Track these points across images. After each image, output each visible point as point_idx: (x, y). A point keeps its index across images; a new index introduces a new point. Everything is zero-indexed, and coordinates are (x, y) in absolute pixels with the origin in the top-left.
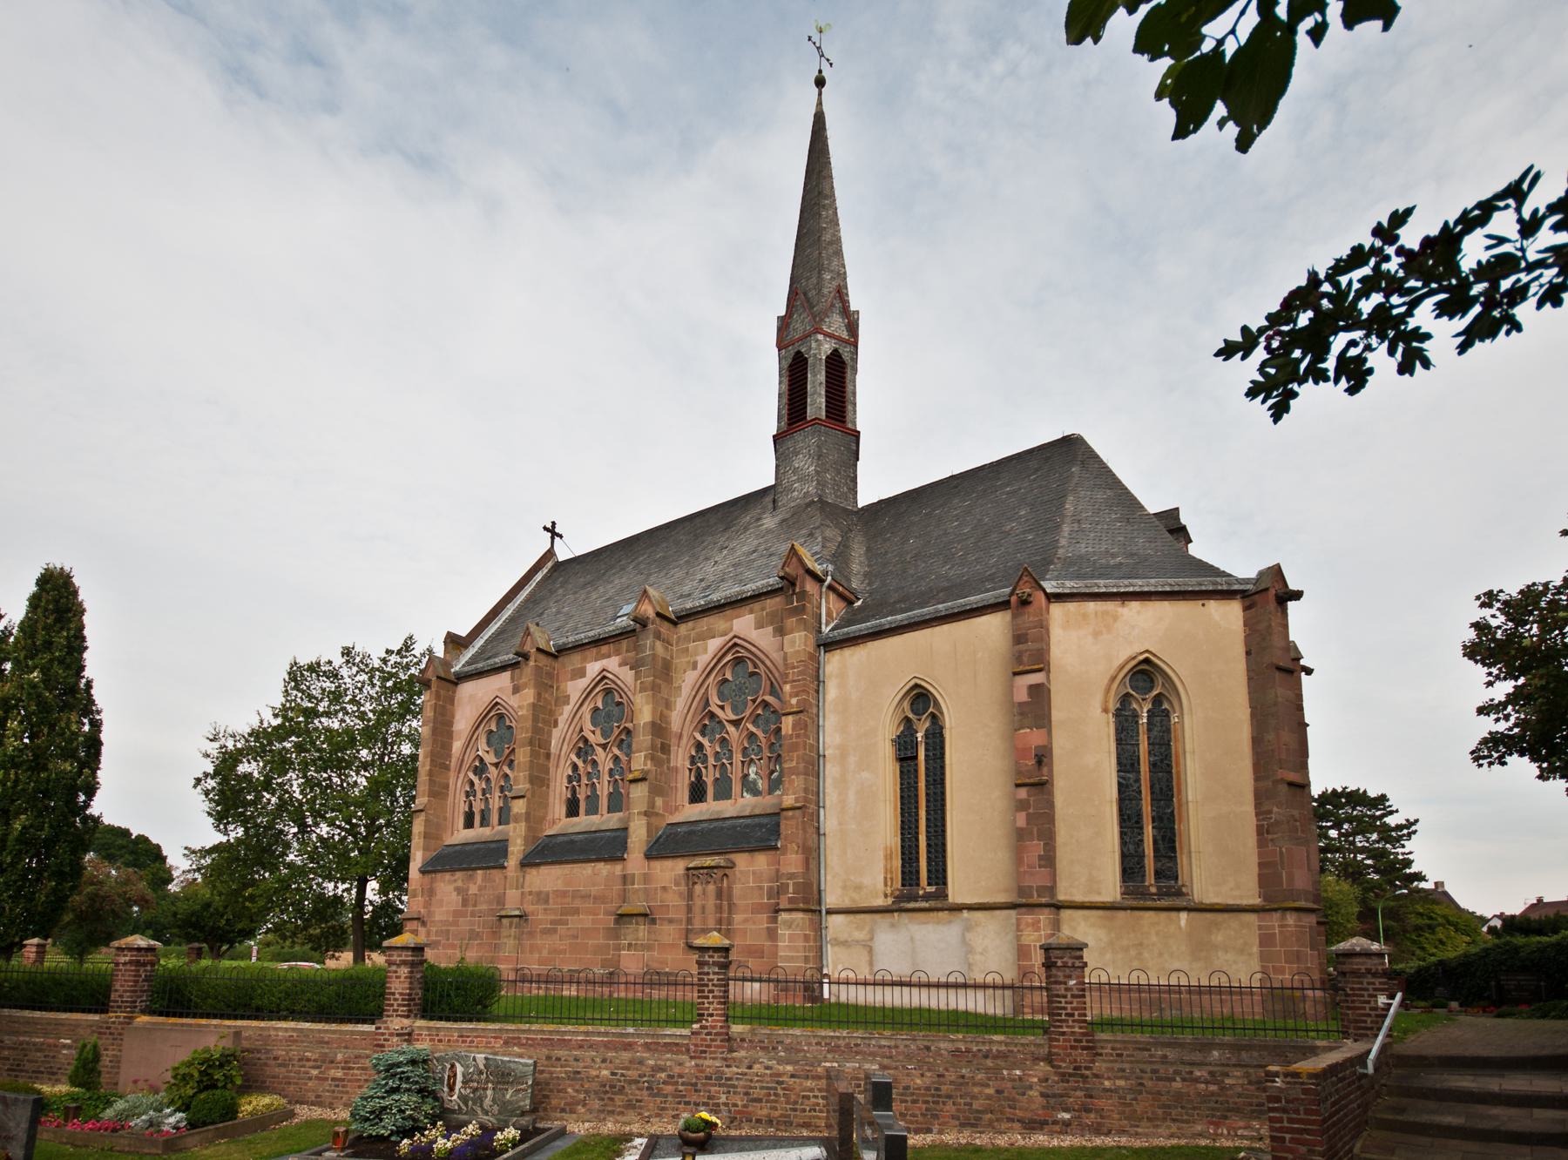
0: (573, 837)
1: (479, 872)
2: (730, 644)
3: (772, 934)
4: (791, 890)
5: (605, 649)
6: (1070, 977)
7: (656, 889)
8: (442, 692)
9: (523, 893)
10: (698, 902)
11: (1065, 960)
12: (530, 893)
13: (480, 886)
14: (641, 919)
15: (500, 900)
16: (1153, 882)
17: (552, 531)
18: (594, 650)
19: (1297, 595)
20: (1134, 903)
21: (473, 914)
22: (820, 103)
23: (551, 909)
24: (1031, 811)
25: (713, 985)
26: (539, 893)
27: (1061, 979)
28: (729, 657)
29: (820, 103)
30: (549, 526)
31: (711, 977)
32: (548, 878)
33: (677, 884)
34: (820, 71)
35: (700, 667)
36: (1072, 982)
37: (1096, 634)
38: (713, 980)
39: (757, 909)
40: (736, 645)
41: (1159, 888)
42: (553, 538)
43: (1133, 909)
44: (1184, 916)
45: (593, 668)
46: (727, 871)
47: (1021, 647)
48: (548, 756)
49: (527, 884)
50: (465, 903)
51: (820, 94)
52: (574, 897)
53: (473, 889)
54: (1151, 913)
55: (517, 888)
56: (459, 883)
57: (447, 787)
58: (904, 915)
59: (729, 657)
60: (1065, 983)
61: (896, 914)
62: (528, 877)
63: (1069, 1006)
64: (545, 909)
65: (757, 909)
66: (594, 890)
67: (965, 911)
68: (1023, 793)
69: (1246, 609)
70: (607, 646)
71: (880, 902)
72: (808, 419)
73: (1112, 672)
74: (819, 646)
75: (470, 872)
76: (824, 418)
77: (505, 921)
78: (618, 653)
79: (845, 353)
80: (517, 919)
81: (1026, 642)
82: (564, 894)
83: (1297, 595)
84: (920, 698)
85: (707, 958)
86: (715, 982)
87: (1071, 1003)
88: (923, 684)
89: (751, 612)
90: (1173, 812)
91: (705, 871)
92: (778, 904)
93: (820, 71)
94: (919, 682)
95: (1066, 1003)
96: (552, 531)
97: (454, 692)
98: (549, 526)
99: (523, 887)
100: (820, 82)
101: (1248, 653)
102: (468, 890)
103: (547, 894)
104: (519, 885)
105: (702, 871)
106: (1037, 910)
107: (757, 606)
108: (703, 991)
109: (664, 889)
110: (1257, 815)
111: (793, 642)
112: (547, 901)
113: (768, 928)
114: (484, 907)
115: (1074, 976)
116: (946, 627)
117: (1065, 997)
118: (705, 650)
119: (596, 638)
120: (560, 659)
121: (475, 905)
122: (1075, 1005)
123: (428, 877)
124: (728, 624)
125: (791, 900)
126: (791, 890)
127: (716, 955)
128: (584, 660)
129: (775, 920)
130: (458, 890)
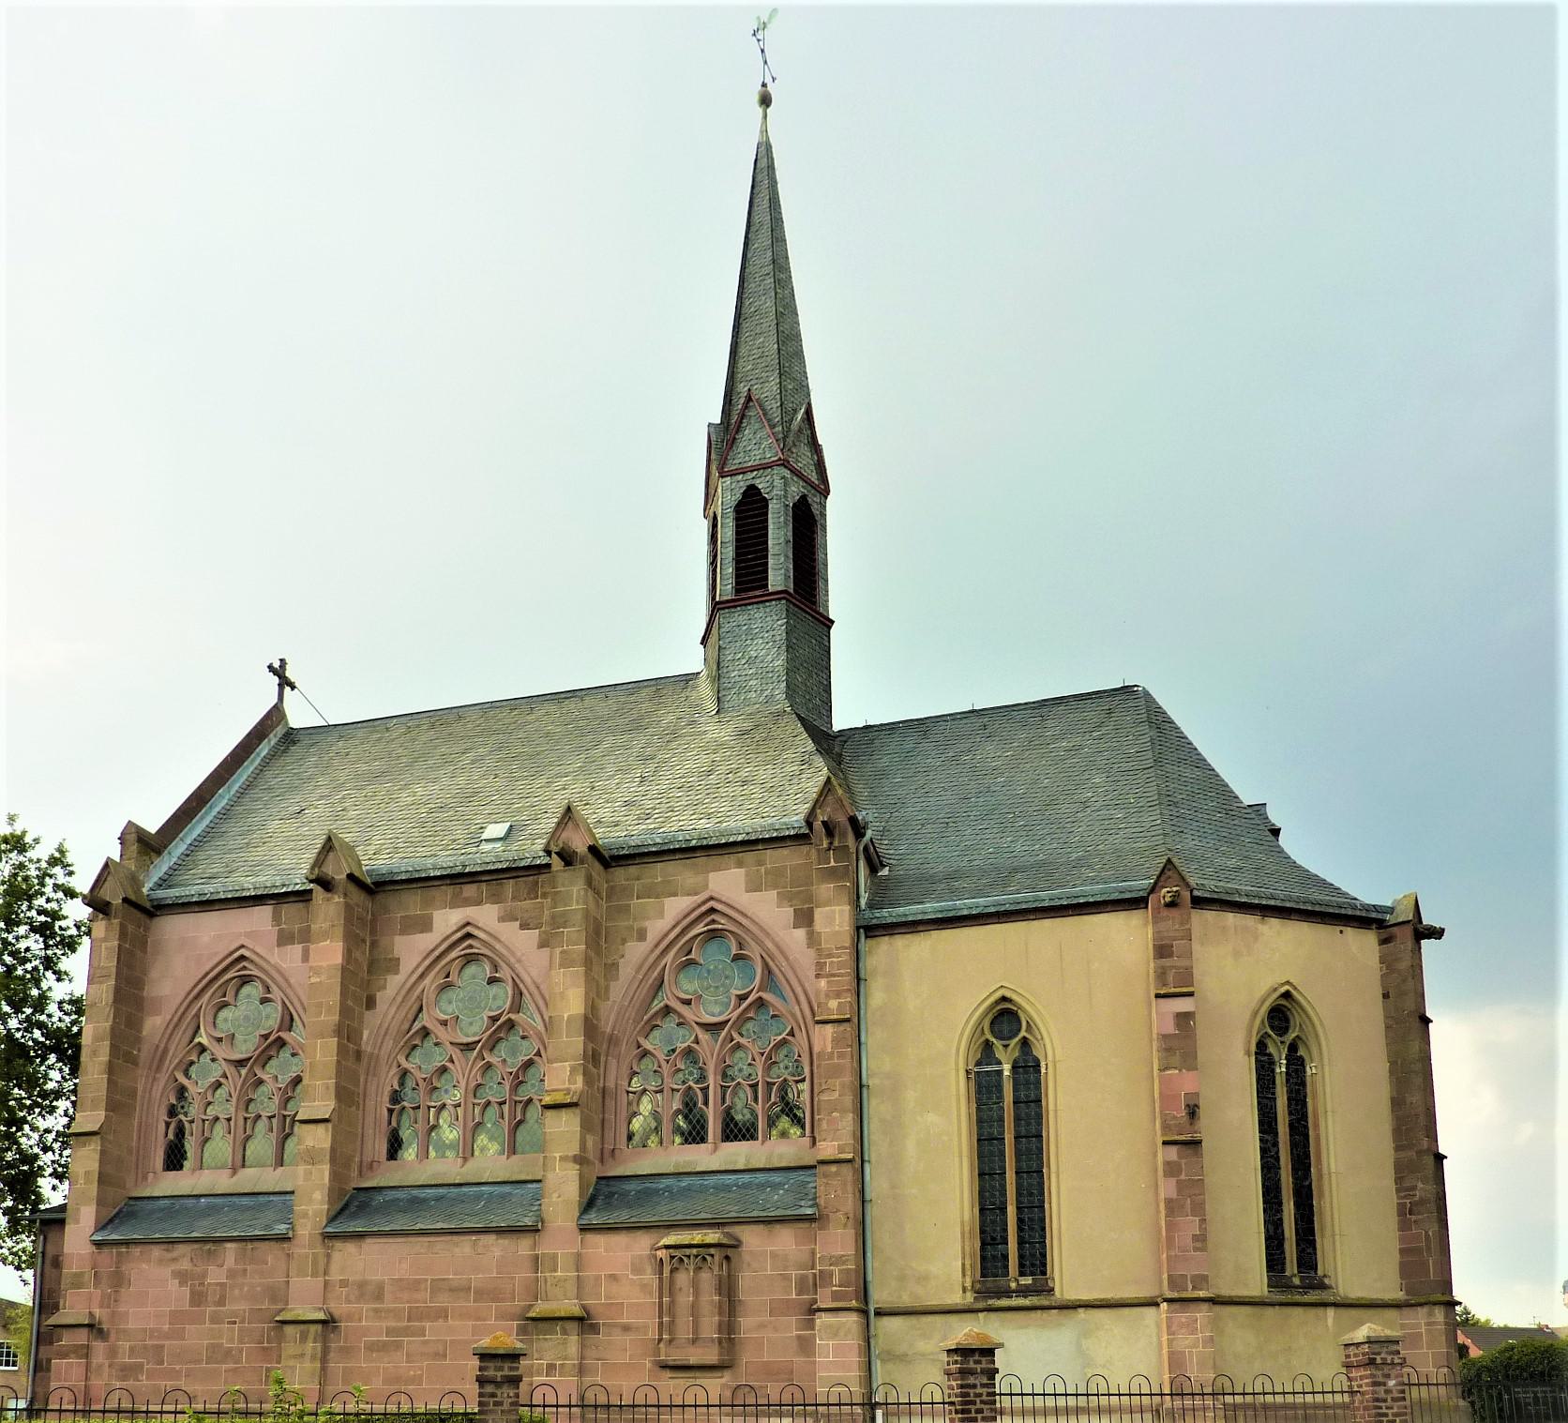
0: (415, 1192)
1: (229, 1245)
2: (704, 908)
3: (806, 1346)
4: (836, 1280)
5: (470, 890)
6: (1388, 1376)
7: (598, 1278)
8: (130, 928)
9: (326, 1284)
10: (685, 1299)
11: (1383, 1356)
12: (344, 1283)
13: (229, 1270)
14: (573, 1326)
15: (278, 1295)
16: (1296, 1272)
17: (279, 671)
18: (450, 890)
19: (1437, 933)
20: (1282, 1298)
21: (216, 1319)
22: (765, 131)
23: (389, 1311)
24: (1183, 1177)
25: (982, 1402)
26: (362, 1285)
27: (1381, 1379)
28: (700, 928)
29: (765, 131)
30: (277, 665)
31: (979, 1390)
33: (637, 1270)
34: (764, 85)
35: (652, 936)
36: (1391, 1383)
37: (1237, 954)
38: (980, 1395)
39: (778, 1309)
40: (712, 910)
41: (1302, 1279)
42: (281, 686)
43: (1282, 1304)
44: (1331, 1312)
45: (447, 920)
46: (730, 1252)
47: (1166, 962)
48: (358, 1055)
49: (334, 1268)
50: (198, 1298)
51: (765, 116)
54: (1299, 1310)
55: (314, 1274)
56: (185, 1265)
57: (133, 1094)
58: (993, 1316)
59: (700, 928)
60: (1385, 1384)
61: (981, 1315)
62: (336, 1256)
63: (1390, 1412)
64: (376, 1311)
65: (778, 1309)
66: (477, 1279)
67: (1081, 1310)
68: (1173, 1153)
69: (1384, 941)
70: (474, 886)
71: (956, 1298)
72: (771, 589)
73: (1253, 1005)
74: (858, 928)
75: (208, 1246)
76: (792, 591)
77: (289, 1330)
78: (496, 898)
79: (814, 500)
80: (319, 1327)
81: (1171, 955)
82: (415, 1285)
83: (1437, 933)
84: (1005, 1017)
85: (972, 1365)
86: (984, 1398)
87: (1392, 1408)
88: (1014, 997)
89: (740, 865)
90: (1311, 1184)
91: (695, 1251)
92: (815, 1301)
93: (764, 85)
94: (1008, 994)
95: (1387, 1408)
96: (279, 671)
97: (147, 929)
98: (277, 665)
100: (765, 101)
101: (1386, 996)
102: (204, 1275)
105: (688, 1251)
106: (1192, 1306)
107: (749, 857)
108: (969, 1411)
109: (613, 1278)
110: (1398, 1191)
111: (830, 919)
112: (379, 1296)
113: (799, 1337)
114: (242, 1306)
115: (1392, 1376)
116: (1047, 923)
117: (1385, 1401)
118: (661, 914)
119: (459, 869)
120: (379, 897)
121: (221, 1302)
122: (1395, 1410)
123: (107, 1256)
124: (700, 878)
125: (836, 1296)
126: (836, 1280)
127: (983, 1359)
128: (428, 903)
129: (810, 1325)
130: (182, 1277)
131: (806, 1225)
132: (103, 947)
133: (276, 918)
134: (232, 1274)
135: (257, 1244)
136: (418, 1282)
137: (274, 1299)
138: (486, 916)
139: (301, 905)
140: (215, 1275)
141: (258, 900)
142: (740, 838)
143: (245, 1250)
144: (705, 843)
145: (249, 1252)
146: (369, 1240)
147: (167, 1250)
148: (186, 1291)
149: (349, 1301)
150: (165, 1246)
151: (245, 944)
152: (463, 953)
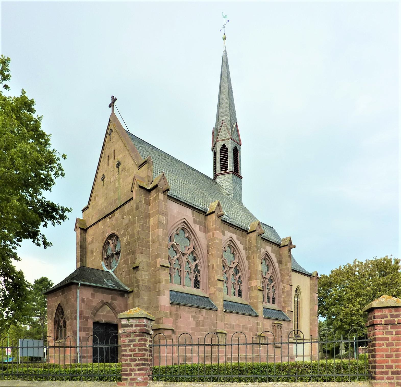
1: (204, 310)
12: (227, 324)
15: (215, 325)
21: (202, 330)
26: (231, 325)
32: (233, 319)
49: (225, 320)
50: (197, 324)
52: (243, 328)
53: (201, 318)
56: (194, 314)
75: (199, 309)
82: (239, 326)
89: (270, 246)
99: (224, 321)
102: (198, 318)
103: (234, 325)
104: (223, 320)
112: (233, 328)
119: (232, 223)
121: (203, 326)
123: (174, 308)
130: (194, 317)
131: (288, 322)
132: (163, 204)
133: (193, 214)
134: (205, 318)
135: (210, 311)
136: (240, 326)
137: (214, 327)
138: (235, 237)
139: (198, 214)
140: (201, 318)
141: (189, 206)
142: (272, 241)
143: (207, 312)
144: (268, 239)
145: (208, 313)
146: (232, 314)
147: (190, 309)
148: (195, 321)
149: (228, 329)
150: (189, 308)
151: (186, 218)
152: (229, 244)
